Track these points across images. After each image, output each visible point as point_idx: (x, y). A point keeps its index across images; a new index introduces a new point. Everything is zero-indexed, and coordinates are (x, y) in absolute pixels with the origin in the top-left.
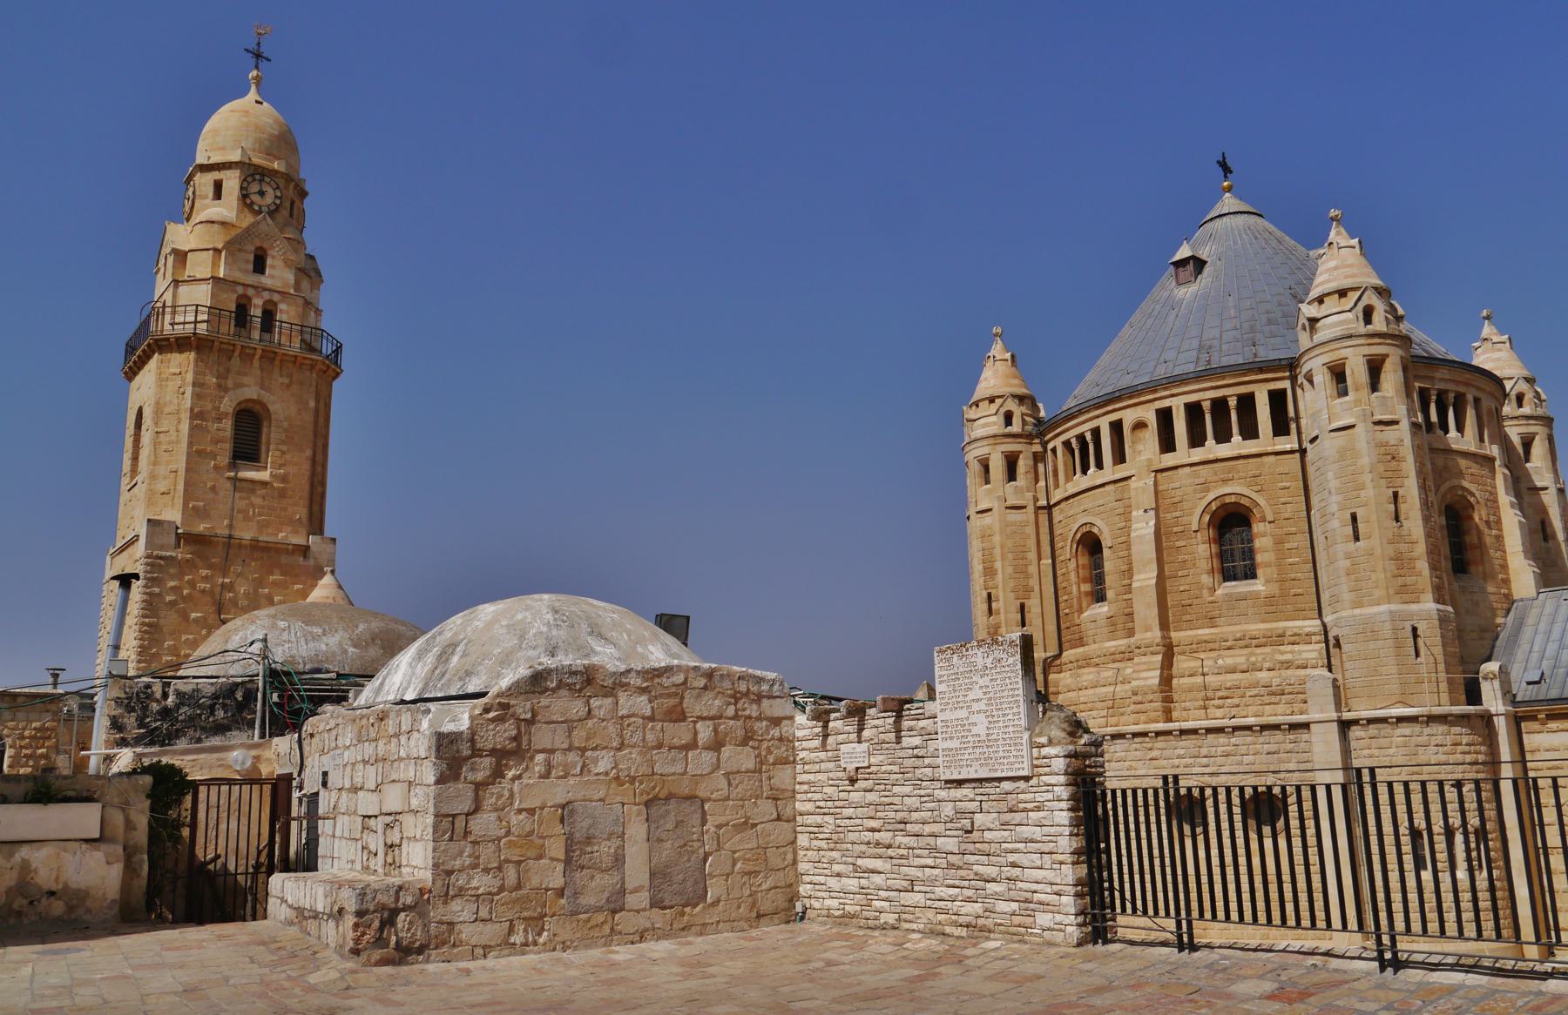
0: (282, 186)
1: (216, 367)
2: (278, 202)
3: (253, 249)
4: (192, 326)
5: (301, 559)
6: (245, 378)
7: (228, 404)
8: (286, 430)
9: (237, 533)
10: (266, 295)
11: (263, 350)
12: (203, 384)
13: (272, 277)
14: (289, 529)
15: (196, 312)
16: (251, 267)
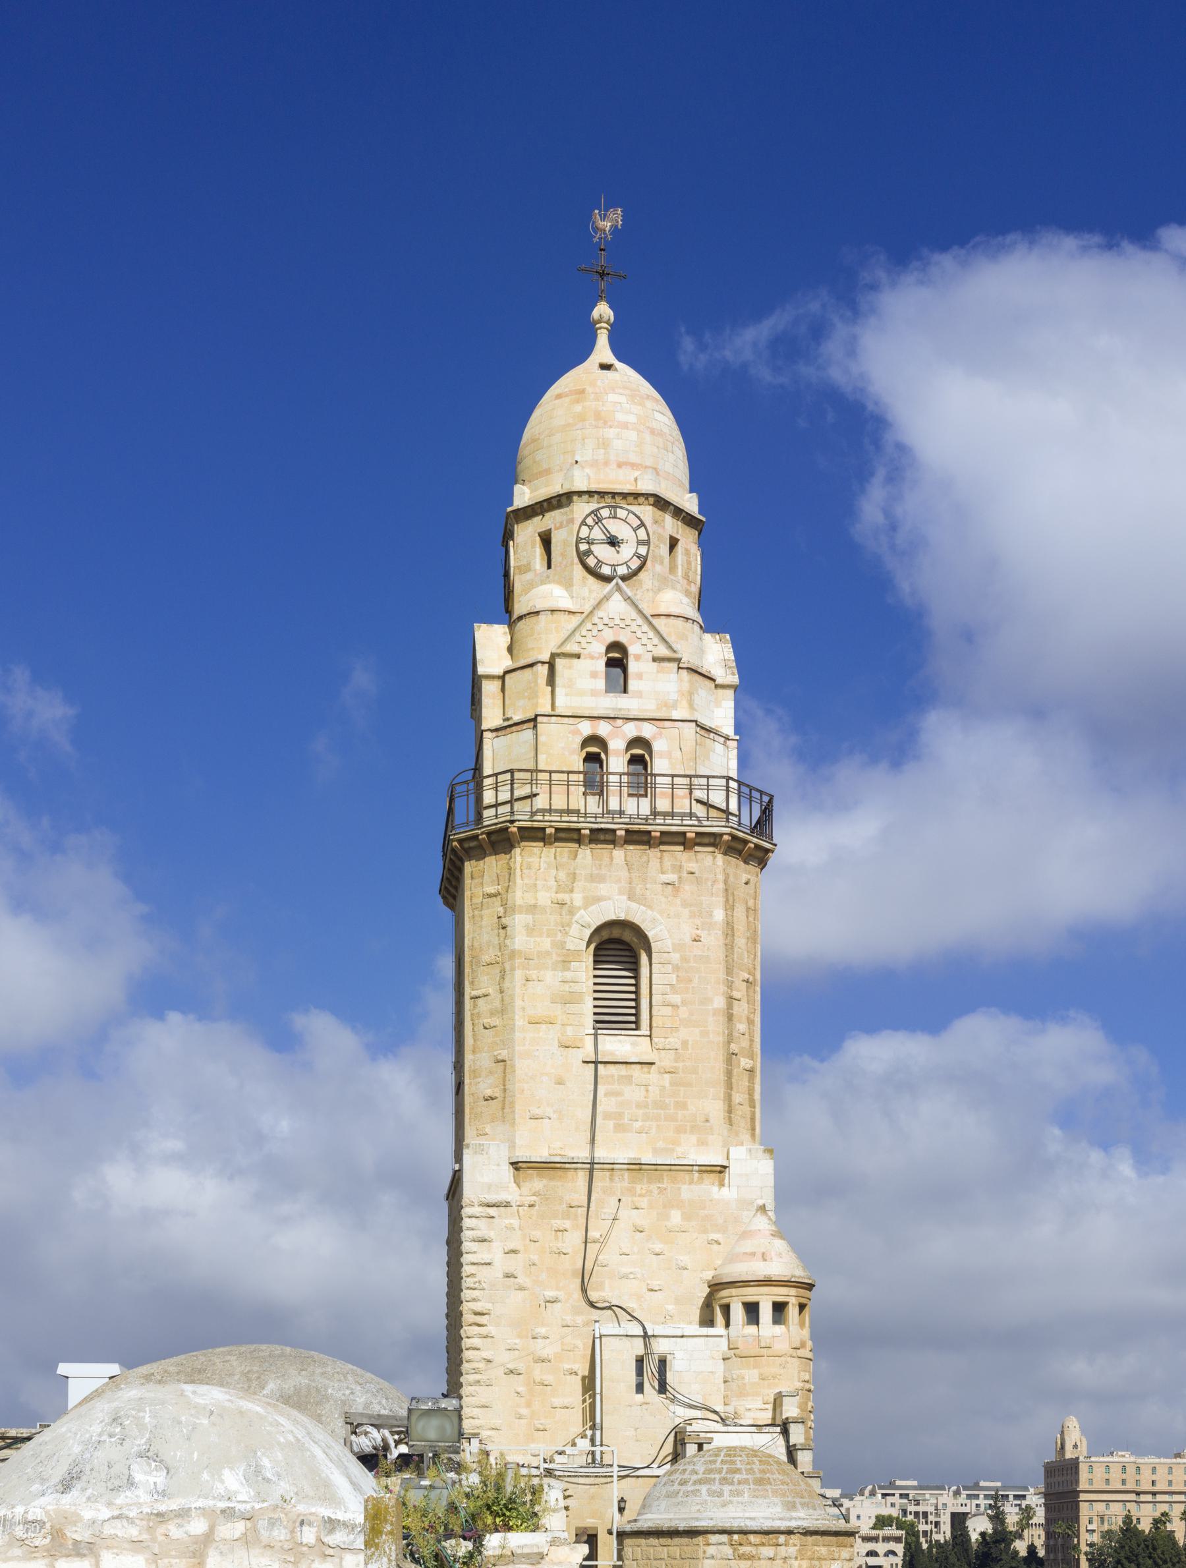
0: (648, 523)
1: (554, 872)
2: (643, 550)
3: (603, 649)
4: (507, 808)
5: (715, 1189)
6: (602, 886)
7: (578, 939)
8: (676, 968)
9: (601, 1154)
10: (632, 730)
11: (627, 831)
12: (535, 906)
13: (639, 694)
14: (693, 1138)
15: (512, 784)
16: (601, 684)
